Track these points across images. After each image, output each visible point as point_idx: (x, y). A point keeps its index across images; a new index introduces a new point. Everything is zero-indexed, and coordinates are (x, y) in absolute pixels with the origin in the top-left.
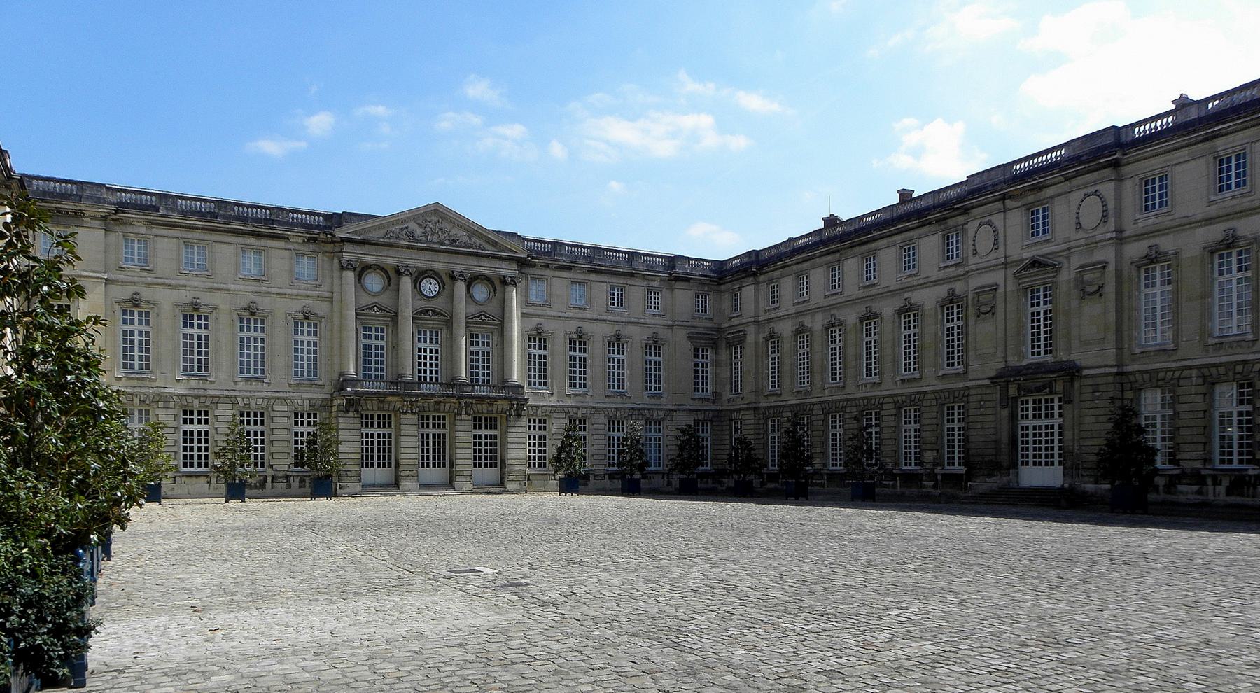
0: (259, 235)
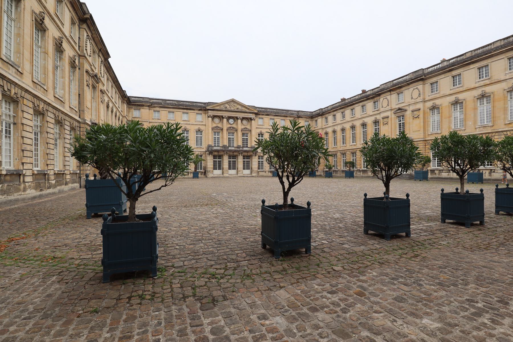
0: (187, 109)
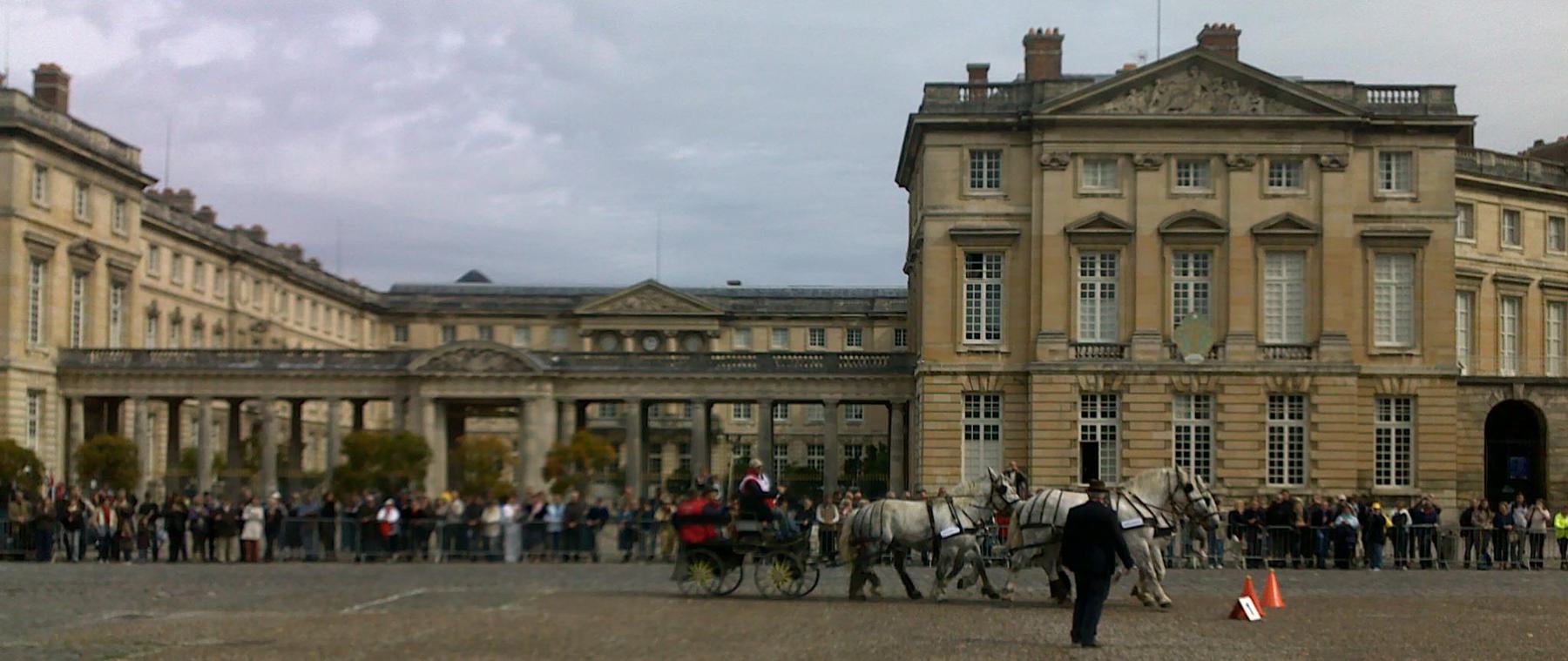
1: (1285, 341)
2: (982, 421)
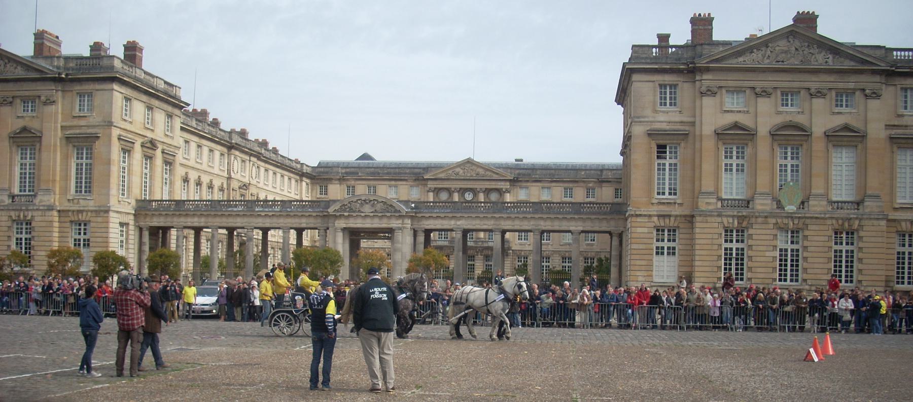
0: (395, 180)
1: (844, 199)
2: (666, 244)
